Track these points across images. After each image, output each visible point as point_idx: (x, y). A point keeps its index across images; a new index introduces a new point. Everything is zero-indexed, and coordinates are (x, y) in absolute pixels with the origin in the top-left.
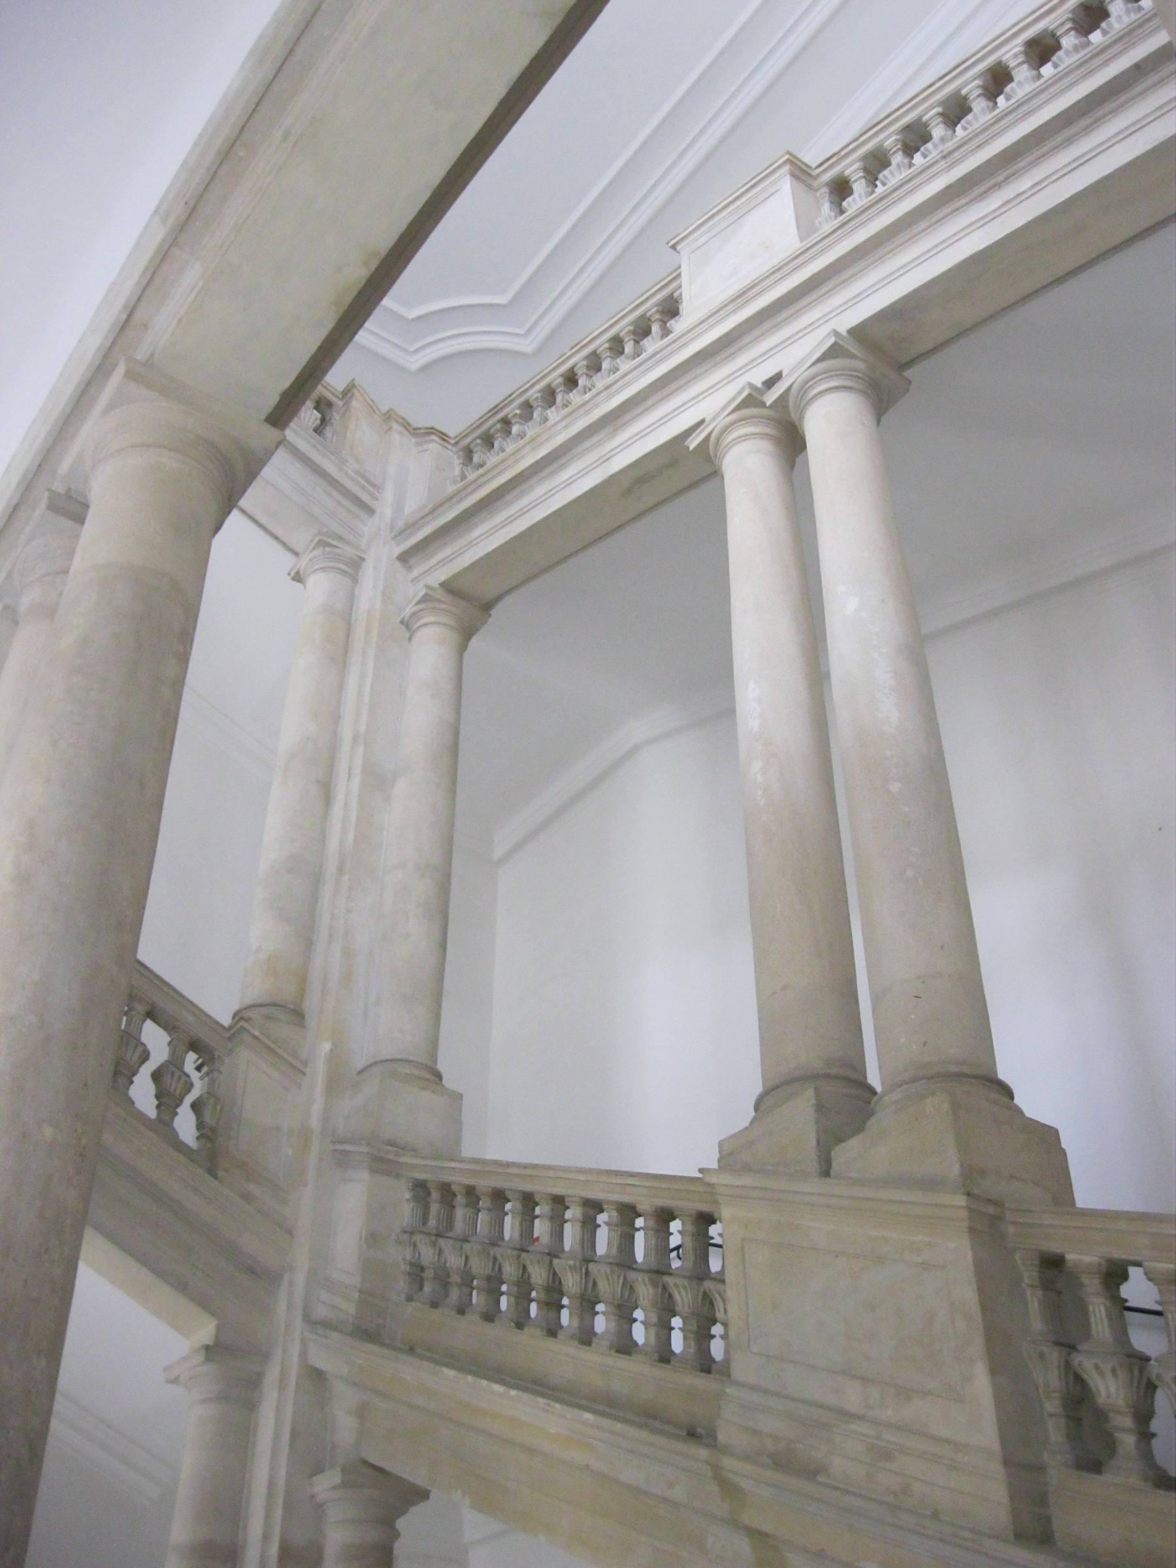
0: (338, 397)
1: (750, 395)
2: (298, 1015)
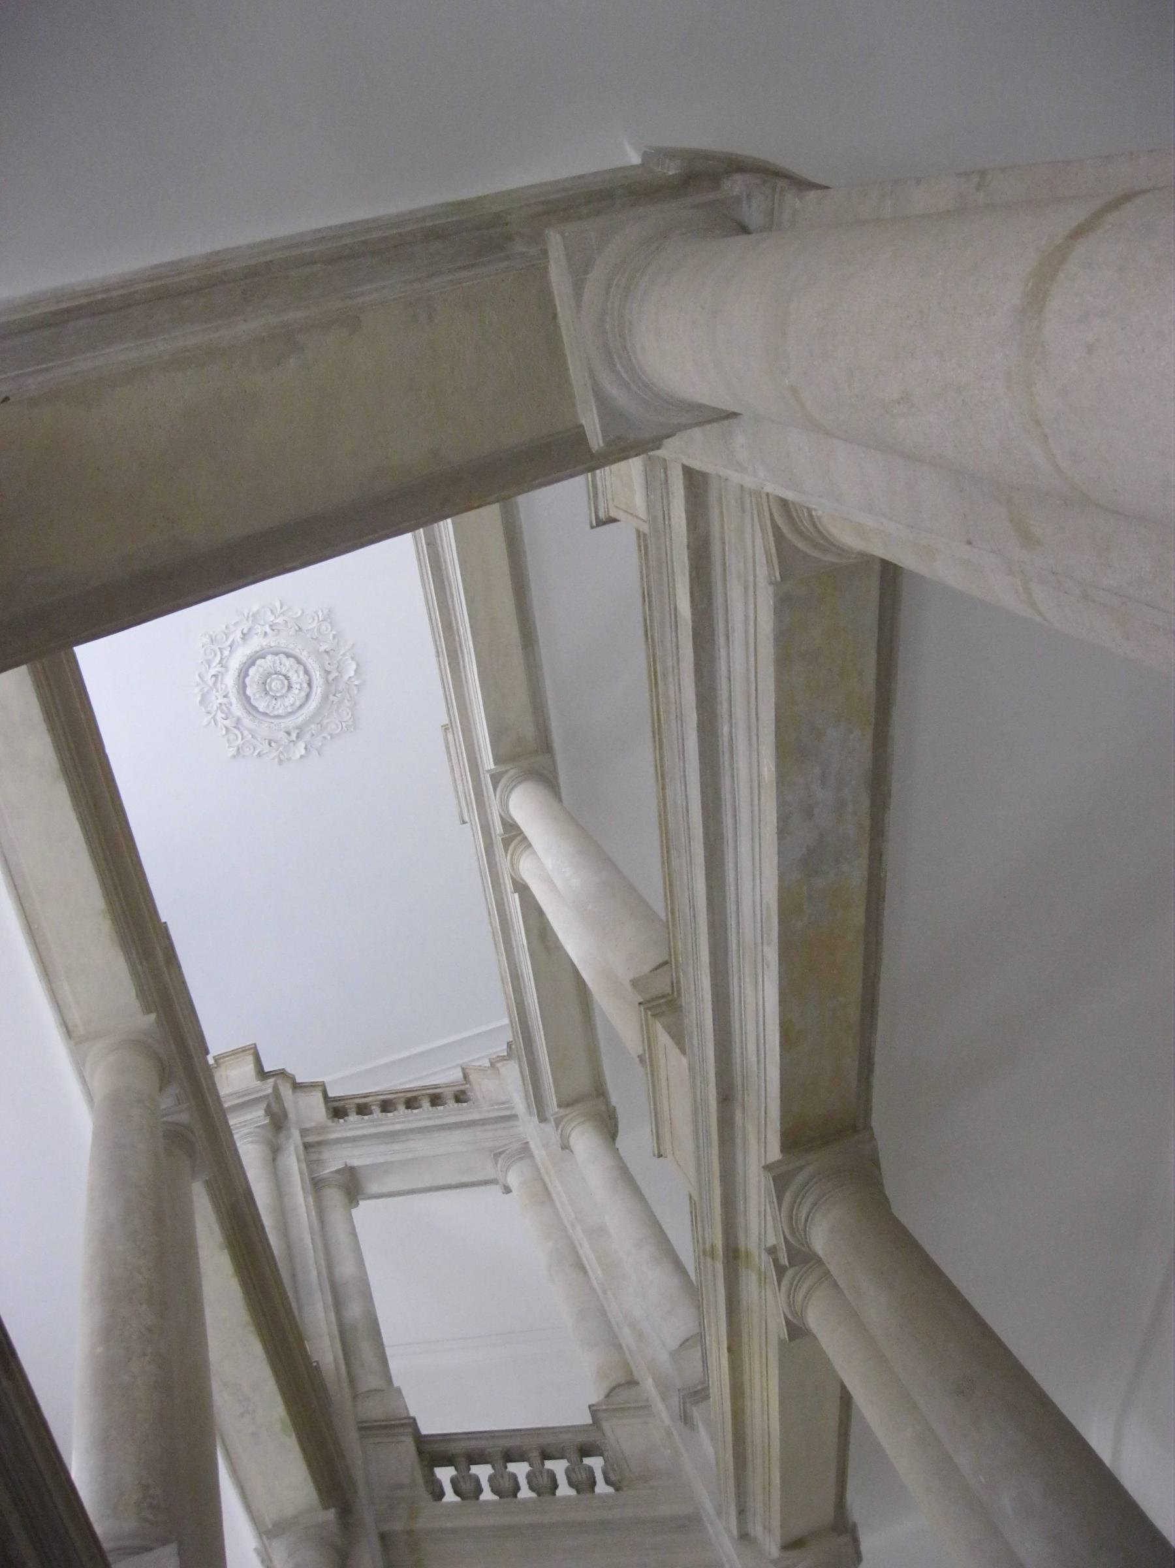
0: (462, 1085)
1: (502, 839)
2: (632, 1383)
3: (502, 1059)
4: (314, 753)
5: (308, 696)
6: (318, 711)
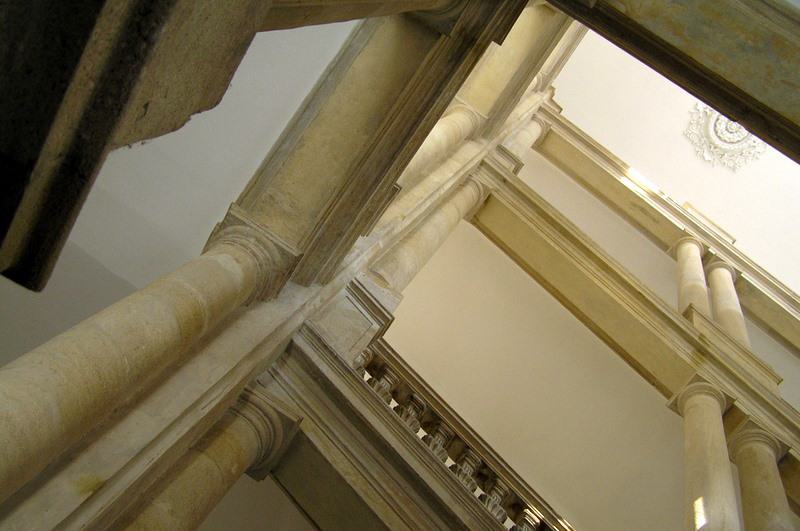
3: (553, 95)
4: (693, 111)
5: (716, 133)
6: (707, 131)
